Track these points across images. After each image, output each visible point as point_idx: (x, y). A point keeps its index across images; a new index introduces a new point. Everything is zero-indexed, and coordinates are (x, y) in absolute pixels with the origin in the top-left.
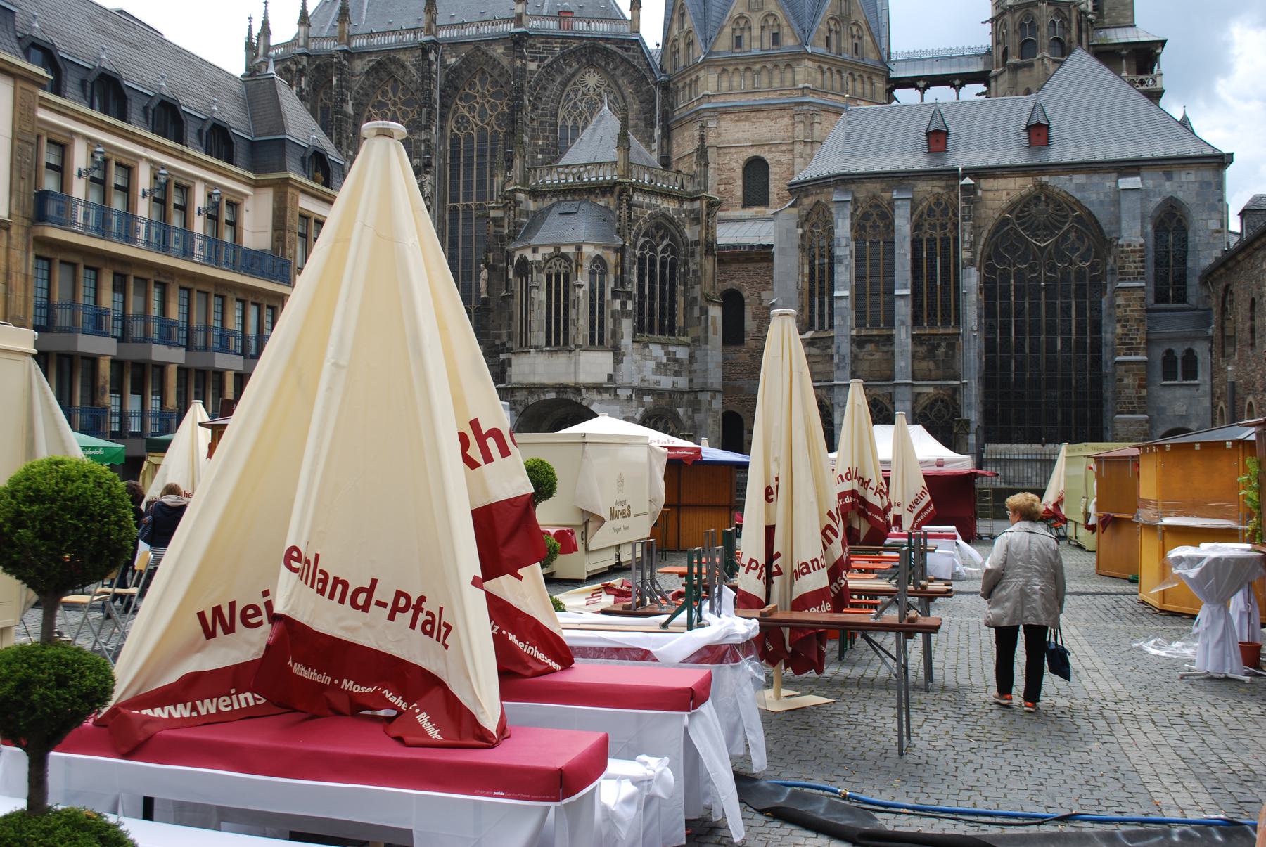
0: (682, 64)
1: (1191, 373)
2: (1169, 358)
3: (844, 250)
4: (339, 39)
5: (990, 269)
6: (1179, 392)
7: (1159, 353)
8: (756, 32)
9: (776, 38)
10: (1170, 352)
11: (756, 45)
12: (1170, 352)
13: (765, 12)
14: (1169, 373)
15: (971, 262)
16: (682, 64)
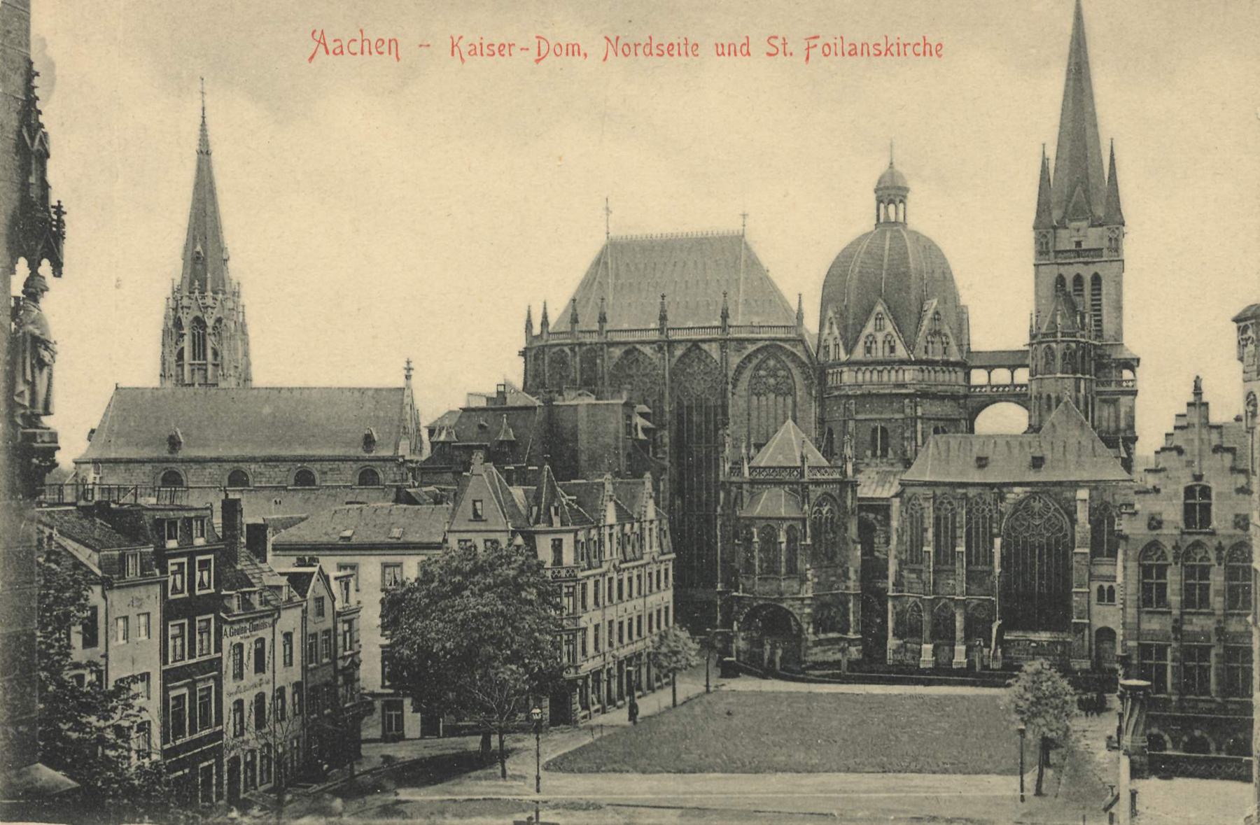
0: (832, 357)
1: (1111, 598)
2: (1101, 589)
3: (929, 522)
4: (600, 332)
5: (1009, 535)
6: (1106, 608)
7: (1095, 586)
8: (880, 345)
9: (892, 349)
10: (1101, 587)
11: (880, 354)
12: (1101, 587)
13: (886, 332)
14: (1101, 598)
15: (998, 535)
16: (832, 357)
